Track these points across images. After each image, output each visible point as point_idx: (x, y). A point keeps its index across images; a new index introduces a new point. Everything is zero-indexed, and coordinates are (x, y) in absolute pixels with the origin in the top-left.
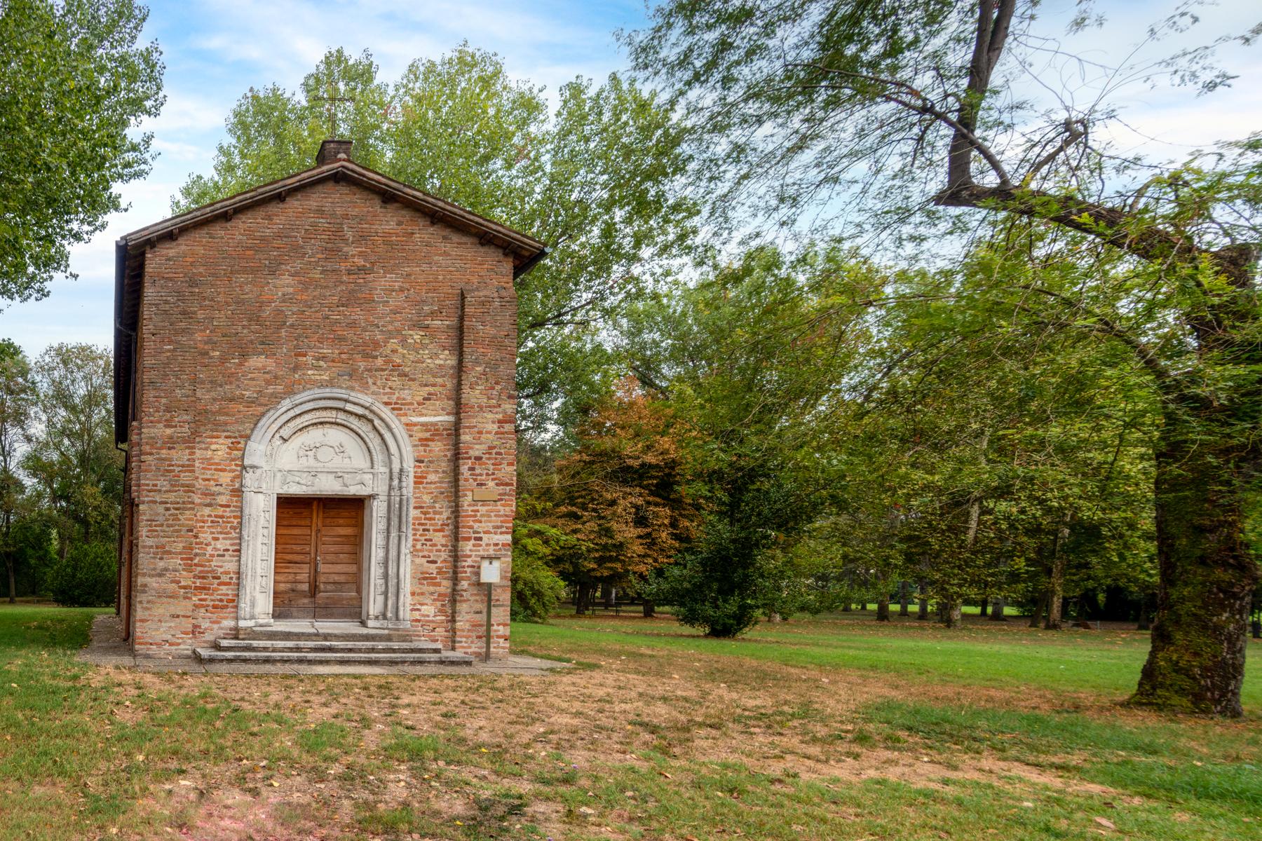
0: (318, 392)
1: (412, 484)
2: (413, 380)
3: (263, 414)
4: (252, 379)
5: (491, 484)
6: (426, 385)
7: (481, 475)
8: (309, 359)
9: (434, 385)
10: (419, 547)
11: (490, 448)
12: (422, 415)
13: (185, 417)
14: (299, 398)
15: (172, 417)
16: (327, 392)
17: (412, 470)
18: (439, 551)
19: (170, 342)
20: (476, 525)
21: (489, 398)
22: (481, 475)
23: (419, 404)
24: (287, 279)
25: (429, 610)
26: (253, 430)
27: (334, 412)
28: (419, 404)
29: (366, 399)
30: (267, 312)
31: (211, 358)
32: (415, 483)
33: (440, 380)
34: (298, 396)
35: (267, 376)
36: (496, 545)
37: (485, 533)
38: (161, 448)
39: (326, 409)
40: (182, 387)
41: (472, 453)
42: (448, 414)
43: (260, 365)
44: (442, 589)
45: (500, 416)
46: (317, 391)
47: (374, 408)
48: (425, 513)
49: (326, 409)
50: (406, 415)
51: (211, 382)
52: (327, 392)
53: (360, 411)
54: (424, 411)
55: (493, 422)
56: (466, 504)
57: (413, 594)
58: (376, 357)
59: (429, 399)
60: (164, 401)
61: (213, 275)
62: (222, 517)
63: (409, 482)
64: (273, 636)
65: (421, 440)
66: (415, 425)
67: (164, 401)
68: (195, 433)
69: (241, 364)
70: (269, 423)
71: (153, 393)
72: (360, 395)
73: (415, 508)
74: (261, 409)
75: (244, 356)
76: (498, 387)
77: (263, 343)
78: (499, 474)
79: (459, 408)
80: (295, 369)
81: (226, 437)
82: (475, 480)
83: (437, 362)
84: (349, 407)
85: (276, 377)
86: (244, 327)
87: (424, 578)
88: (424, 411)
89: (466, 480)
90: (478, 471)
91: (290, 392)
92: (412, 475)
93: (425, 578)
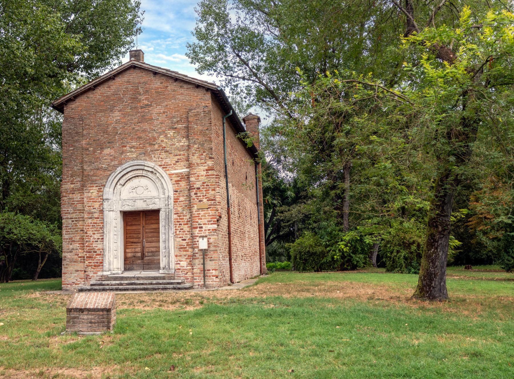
0: (132, 163)
1: (173, 203)
2: (171, 153)
3: (110, 175)
4: (106, 159)
5: (205, 200)
6: (176, 155)
7: (200, 196)
8: (128, 148)
9: (180, 155)
11: (204, 183)
12: (175, 169)
13: (78, 179)
14: (124, 166)
15: (73, 179)
16: (136, 162)
17: (172, 196)
18: (186, 234)
19: (72, 146)
20: (199, 221)
21: (201, 160)
22: (200, 196)
23: (174, 164)
24: (117, 113)
25: (184, 264)
26: (106, 182)
27: (141, 171)
28: (174, 164)
29: (151, 164)
30: (110, 128)
31: (89, 151)
32: (174, 202)
33: (182, 153)
34: (124, 166)
35: (111, 157)
36: (209, 230)
37: (204, 224)
38: (69, 194)
39: (138, 170)
40: (77, 166)
41: (195, 186)
42: (187, 168)
43: (108, 153)
44: (189, 253)
45: (206, 168)
46: (131, 162)
47: (155, 168)
48: (179, 216)
49: (138, 170)
50: (169, 170)
51: (90, 162)
52: (136, 162)
53: (150, 170)
54: (176, 168)
55: (204, 171)
56: (194, 211)
57: (176, 256)
58: (155, 145)
59: (176, 162)
60: (70, 172)
61: (89, 114)
62: (96, 223)
63: (172, 201)
64: (122, 278)
65: (176, 181)
66: (173, 174)
67: (70, 172)
68: (83, 186)
69: (101, 153)
70: (113, 178)
71: (66, 169)
72: (149, 163)
74: (109, 172)
75: (102, 149)
76: (205, 154)
77: (109, 143)
78: (208, 195)
79: (190, 166)
80: (122, 153)
81: (96, 186)
82: (198, 199)
83: (181, 144)
84: (146, 168)
85: (115, 158)
86: (102, 136)
87: (181, 248)
88: (176, 168)
89: (194, 199)
90: (199, 195)
91: (120, 164)
92: (172, 198)
93: (181, 248)
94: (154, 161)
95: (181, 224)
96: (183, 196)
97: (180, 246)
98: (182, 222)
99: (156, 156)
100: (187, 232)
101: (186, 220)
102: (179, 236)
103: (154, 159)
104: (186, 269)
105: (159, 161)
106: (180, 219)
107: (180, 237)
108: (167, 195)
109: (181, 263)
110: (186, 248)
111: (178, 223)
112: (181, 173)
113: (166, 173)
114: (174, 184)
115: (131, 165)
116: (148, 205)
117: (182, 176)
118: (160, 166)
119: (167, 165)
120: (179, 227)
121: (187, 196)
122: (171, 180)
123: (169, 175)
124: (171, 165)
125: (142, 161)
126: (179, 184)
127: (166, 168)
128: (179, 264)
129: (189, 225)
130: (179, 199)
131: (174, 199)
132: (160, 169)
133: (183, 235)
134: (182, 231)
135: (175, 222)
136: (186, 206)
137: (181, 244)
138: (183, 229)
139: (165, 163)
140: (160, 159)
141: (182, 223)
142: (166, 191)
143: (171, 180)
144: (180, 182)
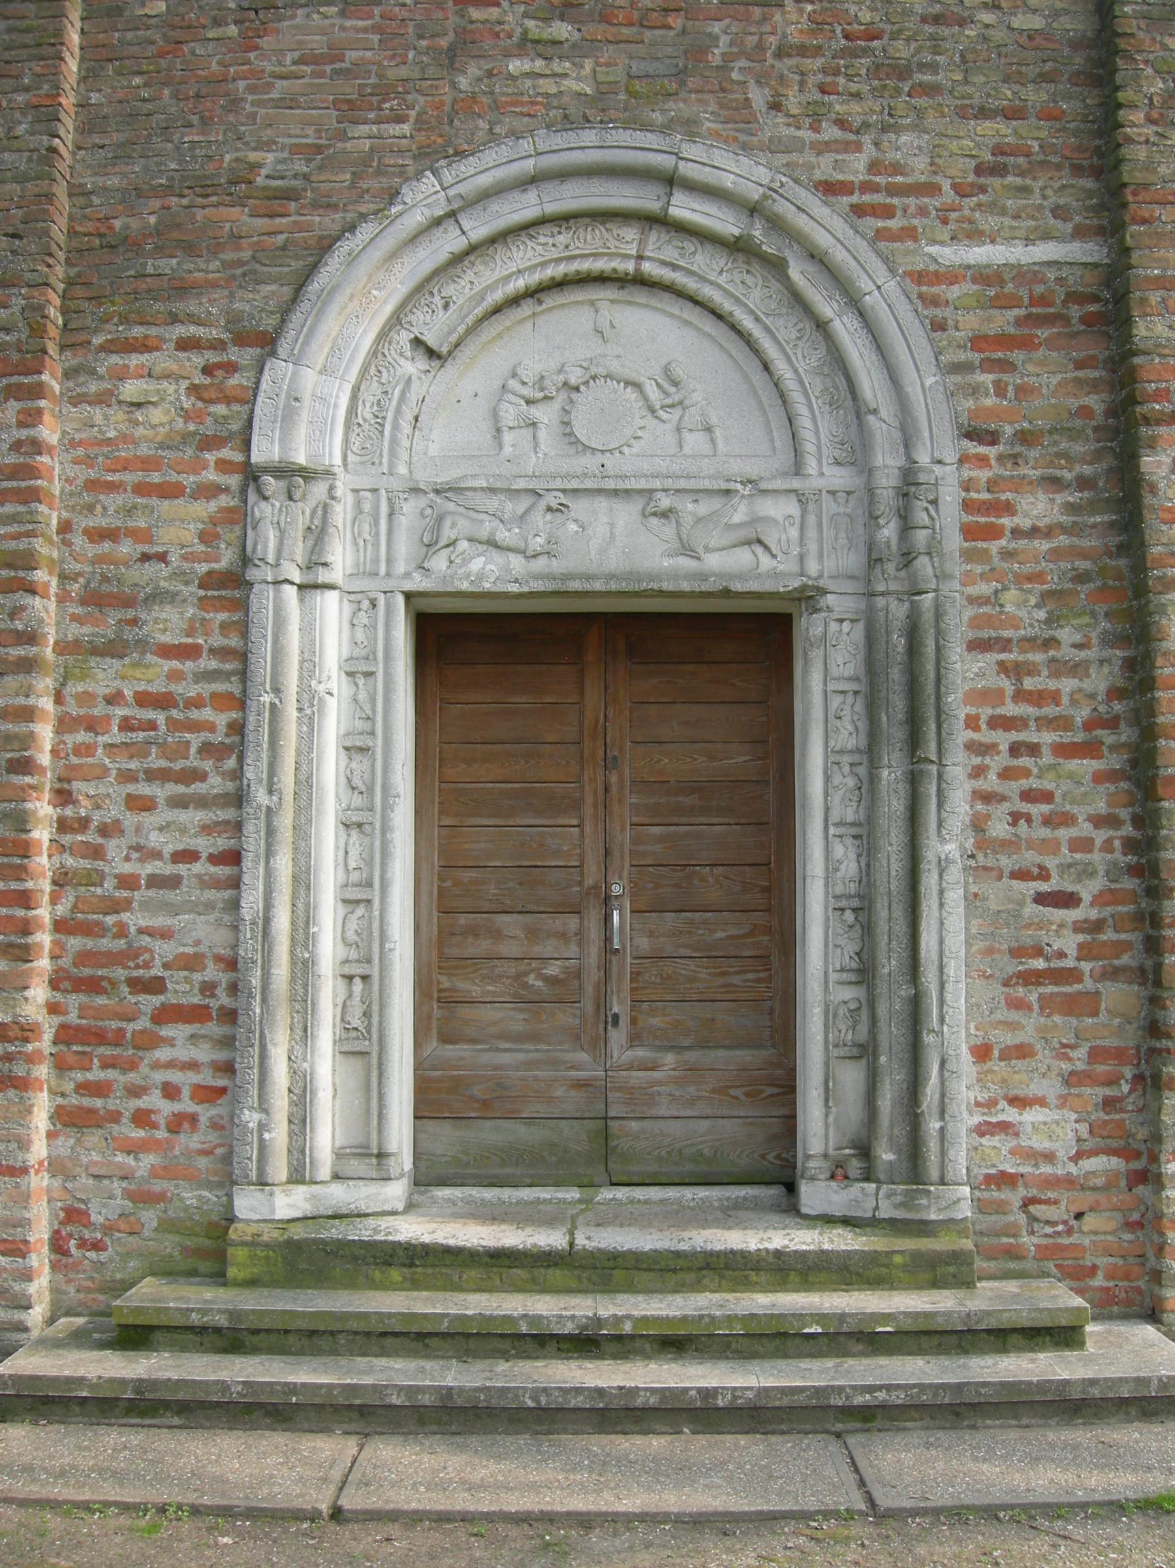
10: (999, 828)
18: (1084, 845)
32: (968, 532)
48: (1016, 671)
50: (910, 233)
73: (978, 646)
93: (1030, 978)
94: (775, 147)
95: (1033, 750)
96: (1054, 483)
97: (1017, 953)
98: (1047, 723)
99: (793, 101)
100: (1085, 828)
101: (1082, 714)
102: (1006, 862)
103: (776, 126)
104: (1069, 1182)
105: (821, 148)
106: (1020, 695)
107: (1021, 875)
108: (887, 462)
109: (1031, 1116)
110: (1073, 975)
111: (1003, 739)
112: (1024, 274)
113: (889, 263)
114: (957, 368)
115: (549, 162)
116: (686, 549)
117: (1042, 301)
118: (829, 189)
119: (892, 190)
120: (1006, 774)
121: (1083, 483)
122: (939, 326)
123: (919, 277)
124: (932, 189)
125: (651, 139)
126: (1006, 366)
127: (888, 212)
128: (1004, 1127)
129: (1115, 762)
130: (1008, 508)
131: (967, 506)
132: (826, 226)
133: (1050, 846)
134: (1037, 810)
135: (972, 723)
136: (1081, 578)
137: (1028, 937)
138: (1048, 797)
139: (874, 166)
140: (831, 132)
141: (1047, 738)
142: (882, 428)
143: (939, 326)
144: (1017, 356)
